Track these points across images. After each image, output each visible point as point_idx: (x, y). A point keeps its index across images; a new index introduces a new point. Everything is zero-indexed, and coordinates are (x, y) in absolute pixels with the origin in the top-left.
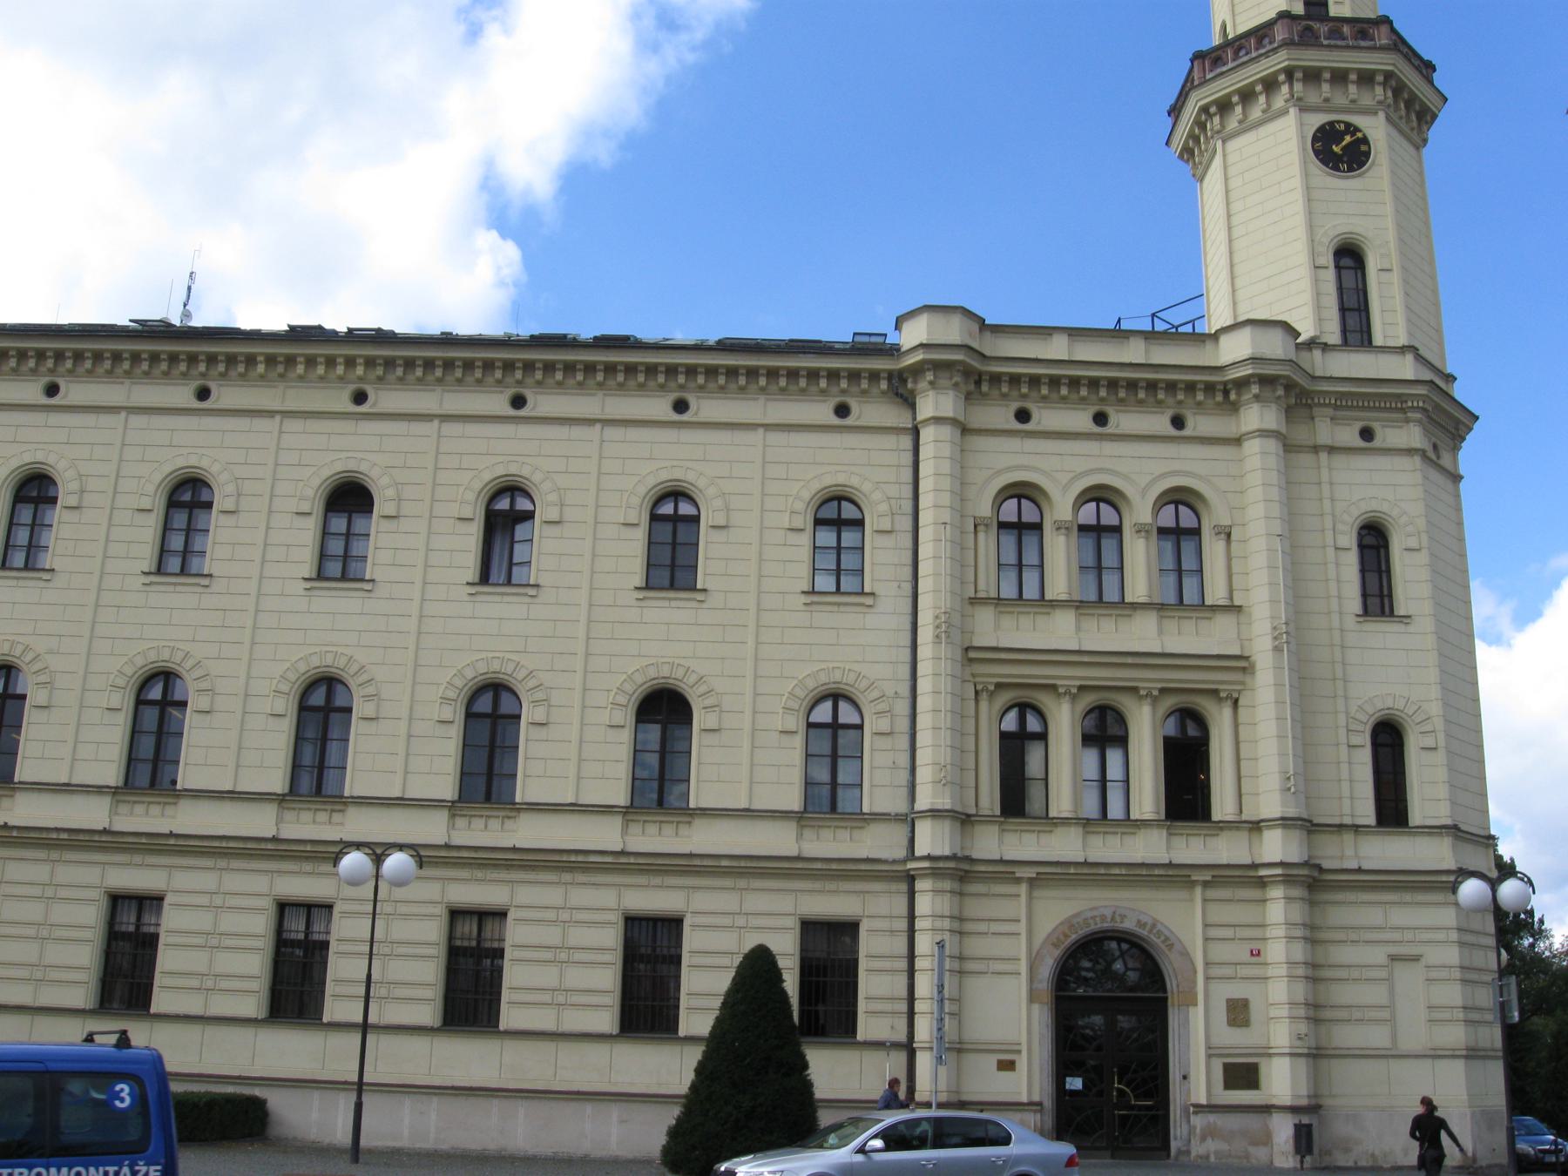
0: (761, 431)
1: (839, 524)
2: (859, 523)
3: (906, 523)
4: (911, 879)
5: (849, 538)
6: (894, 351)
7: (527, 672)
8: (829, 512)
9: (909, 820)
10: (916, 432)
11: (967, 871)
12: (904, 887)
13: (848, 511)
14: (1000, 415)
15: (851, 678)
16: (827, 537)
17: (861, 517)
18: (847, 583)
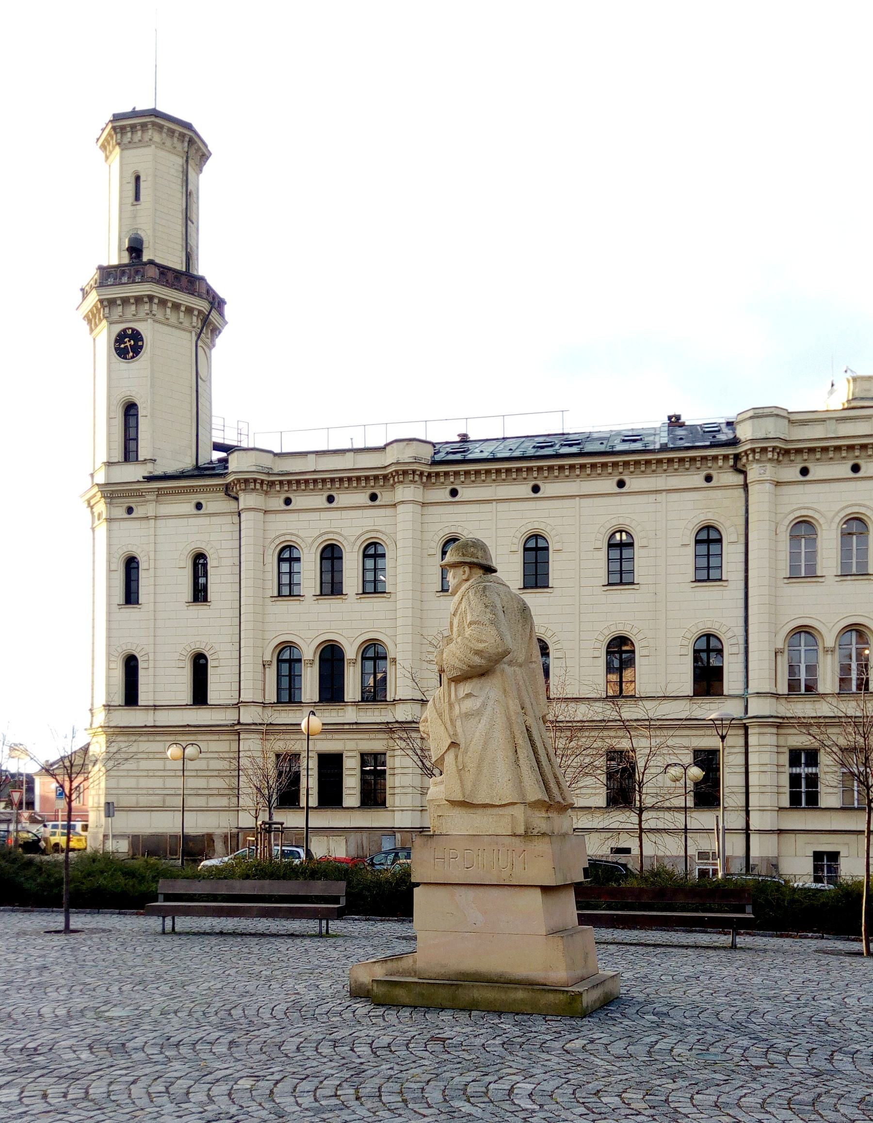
0: (664, 493)
1: (708, 542)
2: (719, 541)
3: (742, 539)
4: (746, 728)
5: (714, 548)
6: (734, 442)
7: (552, 633)
8: (703, 536)
9: (744, 698)
10: (746, 486)
11: (781, 723)
12: (742, 732)
13: (713, 535)
14: (791, 472)
15: (717, 626)
16: (703, 549)
17: (719, 537)
18: (714, 574)
